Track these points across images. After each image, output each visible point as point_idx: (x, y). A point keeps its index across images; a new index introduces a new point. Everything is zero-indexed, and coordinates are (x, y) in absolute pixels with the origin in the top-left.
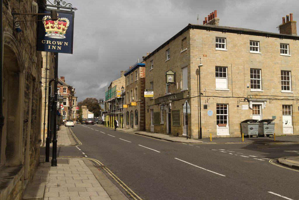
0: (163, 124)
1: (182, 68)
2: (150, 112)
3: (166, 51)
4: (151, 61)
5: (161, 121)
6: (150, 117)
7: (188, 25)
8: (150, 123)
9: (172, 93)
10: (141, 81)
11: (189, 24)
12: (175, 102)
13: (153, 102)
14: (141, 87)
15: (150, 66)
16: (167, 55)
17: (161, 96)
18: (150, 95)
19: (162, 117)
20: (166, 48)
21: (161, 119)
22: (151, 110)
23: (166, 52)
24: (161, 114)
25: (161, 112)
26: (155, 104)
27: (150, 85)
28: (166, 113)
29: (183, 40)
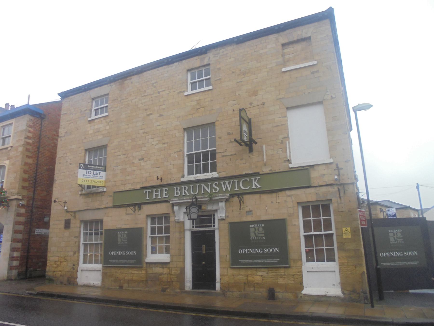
0: (169, 263)
1: (288, 109)
2: (80, 227)
3: (189, 70)
4: (93, 99)
5: (146, 252)
6: (79, 241)
7: (325, 9)
8: (78, 260)
9: (224, 175)
10: (27, 150)
11: (331, 7)
12: (246, 197)
13: (107, 201)
14: (26, 164)
15: (91, 110)
16: (189, 81)
17: (159, 183)
18: (94, 179)
19: (149, 242)
20: (195, 62)
21: (146, 249)
22: (81, 221)
23: (187, 74)
24: (147, 234)
25: (147, 228)
26: (115, 207)
27: (85, 156)
28: (184, 230)
29: (284, 45)
